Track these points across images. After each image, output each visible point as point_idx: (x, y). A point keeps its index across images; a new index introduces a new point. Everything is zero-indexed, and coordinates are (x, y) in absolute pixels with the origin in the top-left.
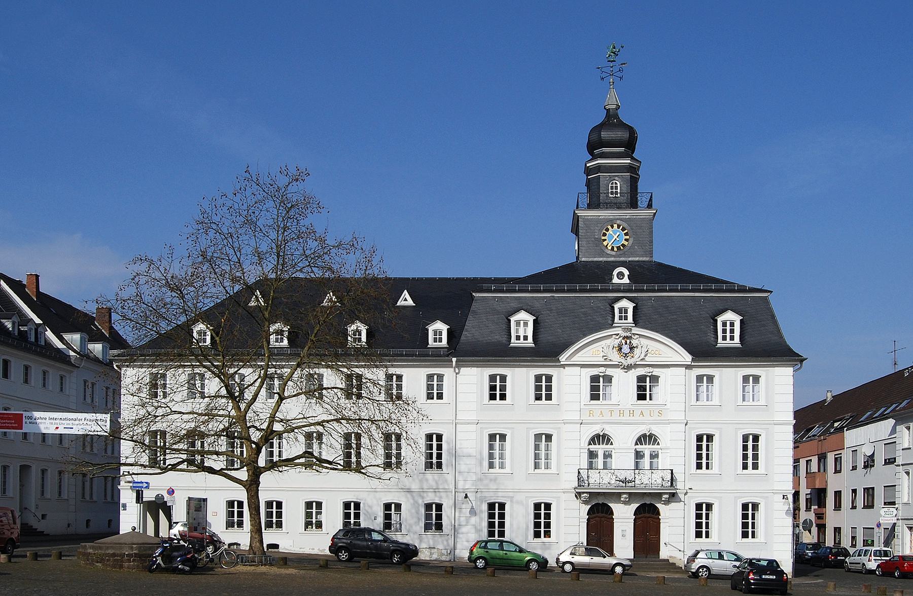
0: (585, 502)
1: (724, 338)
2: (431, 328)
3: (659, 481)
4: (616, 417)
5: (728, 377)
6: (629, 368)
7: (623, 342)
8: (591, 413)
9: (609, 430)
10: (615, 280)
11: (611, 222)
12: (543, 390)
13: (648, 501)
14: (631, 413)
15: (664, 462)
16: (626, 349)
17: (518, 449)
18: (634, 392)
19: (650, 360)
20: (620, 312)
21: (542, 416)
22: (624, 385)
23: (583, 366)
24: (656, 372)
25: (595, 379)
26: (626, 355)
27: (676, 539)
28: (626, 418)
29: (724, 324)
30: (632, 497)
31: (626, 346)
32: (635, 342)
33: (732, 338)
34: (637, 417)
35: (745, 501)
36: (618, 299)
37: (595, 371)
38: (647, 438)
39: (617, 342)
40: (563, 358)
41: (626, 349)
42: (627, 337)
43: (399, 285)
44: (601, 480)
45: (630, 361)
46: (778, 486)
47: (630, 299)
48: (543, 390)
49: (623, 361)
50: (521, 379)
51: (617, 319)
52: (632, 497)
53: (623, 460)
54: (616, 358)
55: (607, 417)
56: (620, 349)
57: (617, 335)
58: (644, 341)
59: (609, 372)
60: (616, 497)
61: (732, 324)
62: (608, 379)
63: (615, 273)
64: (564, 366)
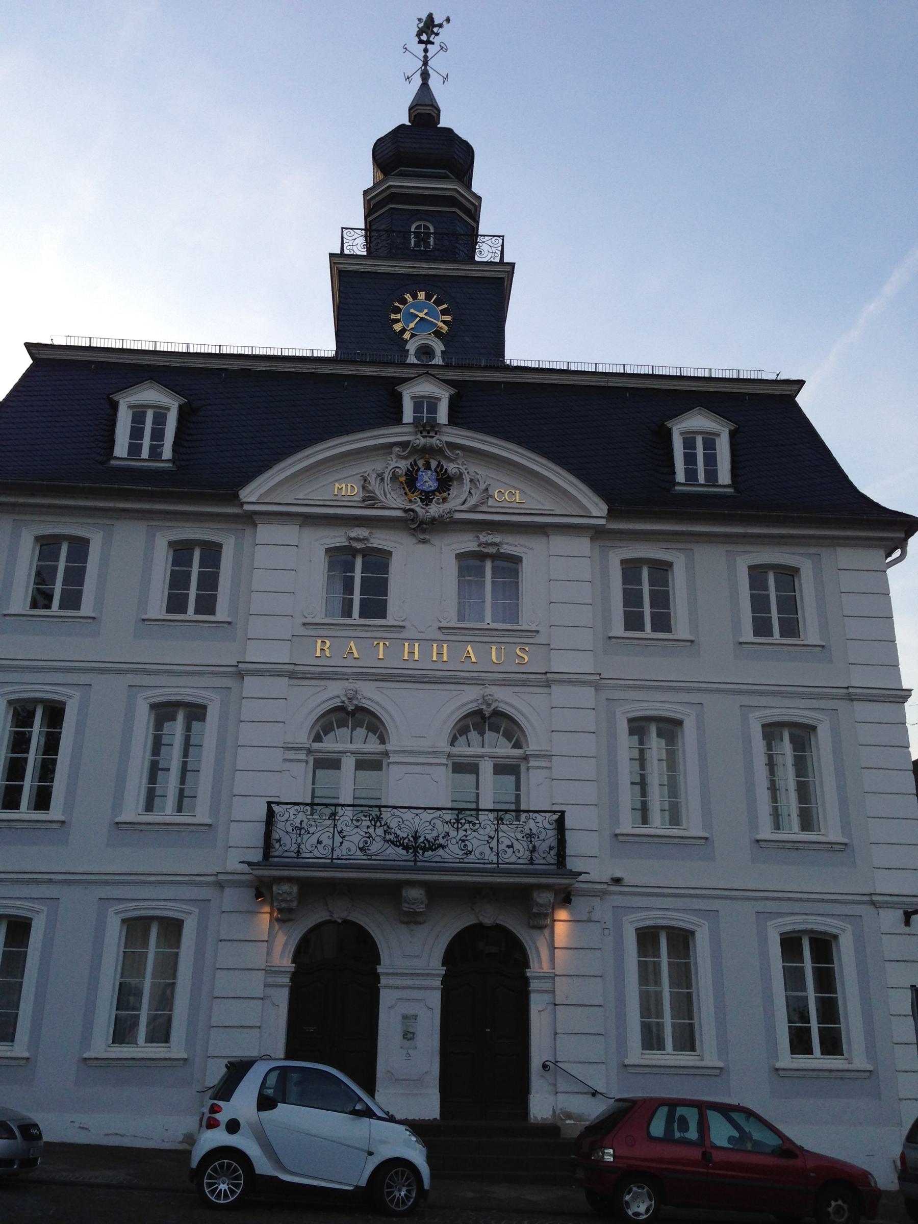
3: (522, 848)
5: (711, 580)
7: (421, 463)
9: (372, 695)
11: (413, 283)
12: (194, 585)
13: (489, 916)
15: (538, 792)
16: (428, 481)
20: (418, 408)
23: (309, 520)
24: (511, 545)
26: (427, 498)
27: (583, 1047)
29: (689, 444)
30: (442, 894)
31: (427, 474)
32: (451, 468)
35: (791, 923)
37: (337, 537)
38: (486, 720)
39: (404, 465)
40: (253, 494)
41: (428, 481)
42: (428, 452)
45: (435, 510)
46: (887, 884)
49: (418, 507)
50: (129, 559)
52: (442, 894)
57: (404, 445)
59: (380, 539)
60: (384, 892)
64: (250, 519)
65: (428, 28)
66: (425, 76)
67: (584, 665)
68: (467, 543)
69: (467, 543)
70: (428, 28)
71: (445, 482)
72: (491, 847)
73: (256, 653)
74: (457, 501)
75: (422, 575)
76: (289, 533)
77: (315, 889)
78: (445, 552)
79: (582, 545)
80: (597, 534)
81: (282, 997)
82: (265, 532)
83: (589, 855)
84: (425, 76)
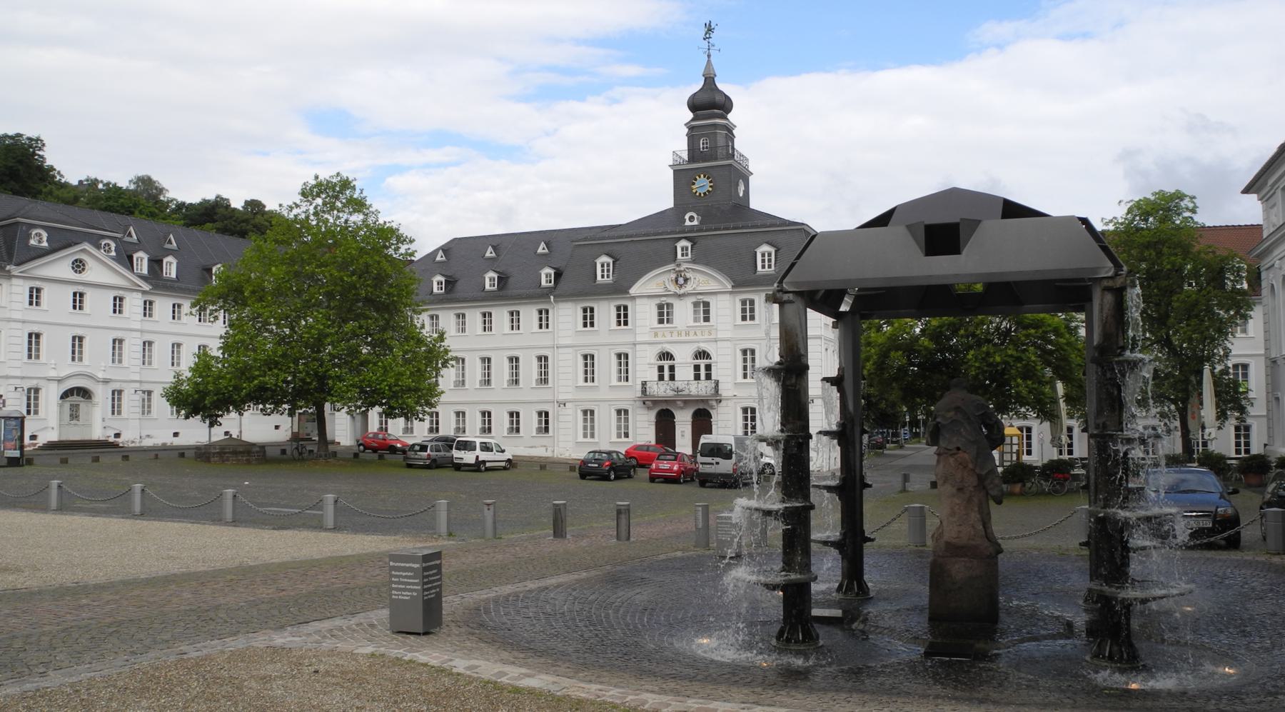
0: (649, 408)
1: (763, 267)
2: (759, 251)
4: (675, 338)
6: (683, 295)
8: (656, 335)
10: (688, 223)
12: (623, 317)
13: (701, 407)
14: (687, 334)
16: (681, 281)
17: (606, 366)
18: (655, 318)
19: (701, 289)
21: (621, 340)
22: (683, 312)
25: (660, 307)
26: (681, 286)
28: (683, 338)
29: (763, 255)
30: (687, 403)
32: (688, 275)
33: (770, 266)
34: (692, 337)
36: (680, 239)
37: (658, 301)
39: (674, 276)
41: (681, 281)
43: (435, 252)
44: (661, 390)
45: (682, 291)
47: (687, 239)
48: (623, 317)
50: (605, 311)
51: (679, 256)
52: (687, 403)
53: (684, 373)
54: (673, 288)
55: (669, 338)
56: (677, 281)
58: (699, 276)
59: (669, 300)
61: (770, 255)
62: (669, 306)
63: (687, 217)
64: (634, 298)
65: (709, 29)
66: (709, 56)
67: (728, 335)
68: (694, 299)
69: (694, 299)
70: (709, 29)
71: (686, 280)
72: (701, 389)
73: (639, 339)
74: (689, 288)
75: (683, 312)
76: (645, 301)
77: (655, 403)
78: (688, 303)
79: (727, 297)
80: (731, 293)
81: (653, 428)
82: (638, 301)
83: (725, 390)
84: (709, 56)
